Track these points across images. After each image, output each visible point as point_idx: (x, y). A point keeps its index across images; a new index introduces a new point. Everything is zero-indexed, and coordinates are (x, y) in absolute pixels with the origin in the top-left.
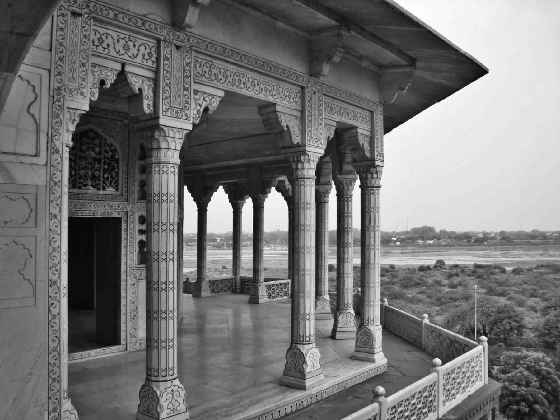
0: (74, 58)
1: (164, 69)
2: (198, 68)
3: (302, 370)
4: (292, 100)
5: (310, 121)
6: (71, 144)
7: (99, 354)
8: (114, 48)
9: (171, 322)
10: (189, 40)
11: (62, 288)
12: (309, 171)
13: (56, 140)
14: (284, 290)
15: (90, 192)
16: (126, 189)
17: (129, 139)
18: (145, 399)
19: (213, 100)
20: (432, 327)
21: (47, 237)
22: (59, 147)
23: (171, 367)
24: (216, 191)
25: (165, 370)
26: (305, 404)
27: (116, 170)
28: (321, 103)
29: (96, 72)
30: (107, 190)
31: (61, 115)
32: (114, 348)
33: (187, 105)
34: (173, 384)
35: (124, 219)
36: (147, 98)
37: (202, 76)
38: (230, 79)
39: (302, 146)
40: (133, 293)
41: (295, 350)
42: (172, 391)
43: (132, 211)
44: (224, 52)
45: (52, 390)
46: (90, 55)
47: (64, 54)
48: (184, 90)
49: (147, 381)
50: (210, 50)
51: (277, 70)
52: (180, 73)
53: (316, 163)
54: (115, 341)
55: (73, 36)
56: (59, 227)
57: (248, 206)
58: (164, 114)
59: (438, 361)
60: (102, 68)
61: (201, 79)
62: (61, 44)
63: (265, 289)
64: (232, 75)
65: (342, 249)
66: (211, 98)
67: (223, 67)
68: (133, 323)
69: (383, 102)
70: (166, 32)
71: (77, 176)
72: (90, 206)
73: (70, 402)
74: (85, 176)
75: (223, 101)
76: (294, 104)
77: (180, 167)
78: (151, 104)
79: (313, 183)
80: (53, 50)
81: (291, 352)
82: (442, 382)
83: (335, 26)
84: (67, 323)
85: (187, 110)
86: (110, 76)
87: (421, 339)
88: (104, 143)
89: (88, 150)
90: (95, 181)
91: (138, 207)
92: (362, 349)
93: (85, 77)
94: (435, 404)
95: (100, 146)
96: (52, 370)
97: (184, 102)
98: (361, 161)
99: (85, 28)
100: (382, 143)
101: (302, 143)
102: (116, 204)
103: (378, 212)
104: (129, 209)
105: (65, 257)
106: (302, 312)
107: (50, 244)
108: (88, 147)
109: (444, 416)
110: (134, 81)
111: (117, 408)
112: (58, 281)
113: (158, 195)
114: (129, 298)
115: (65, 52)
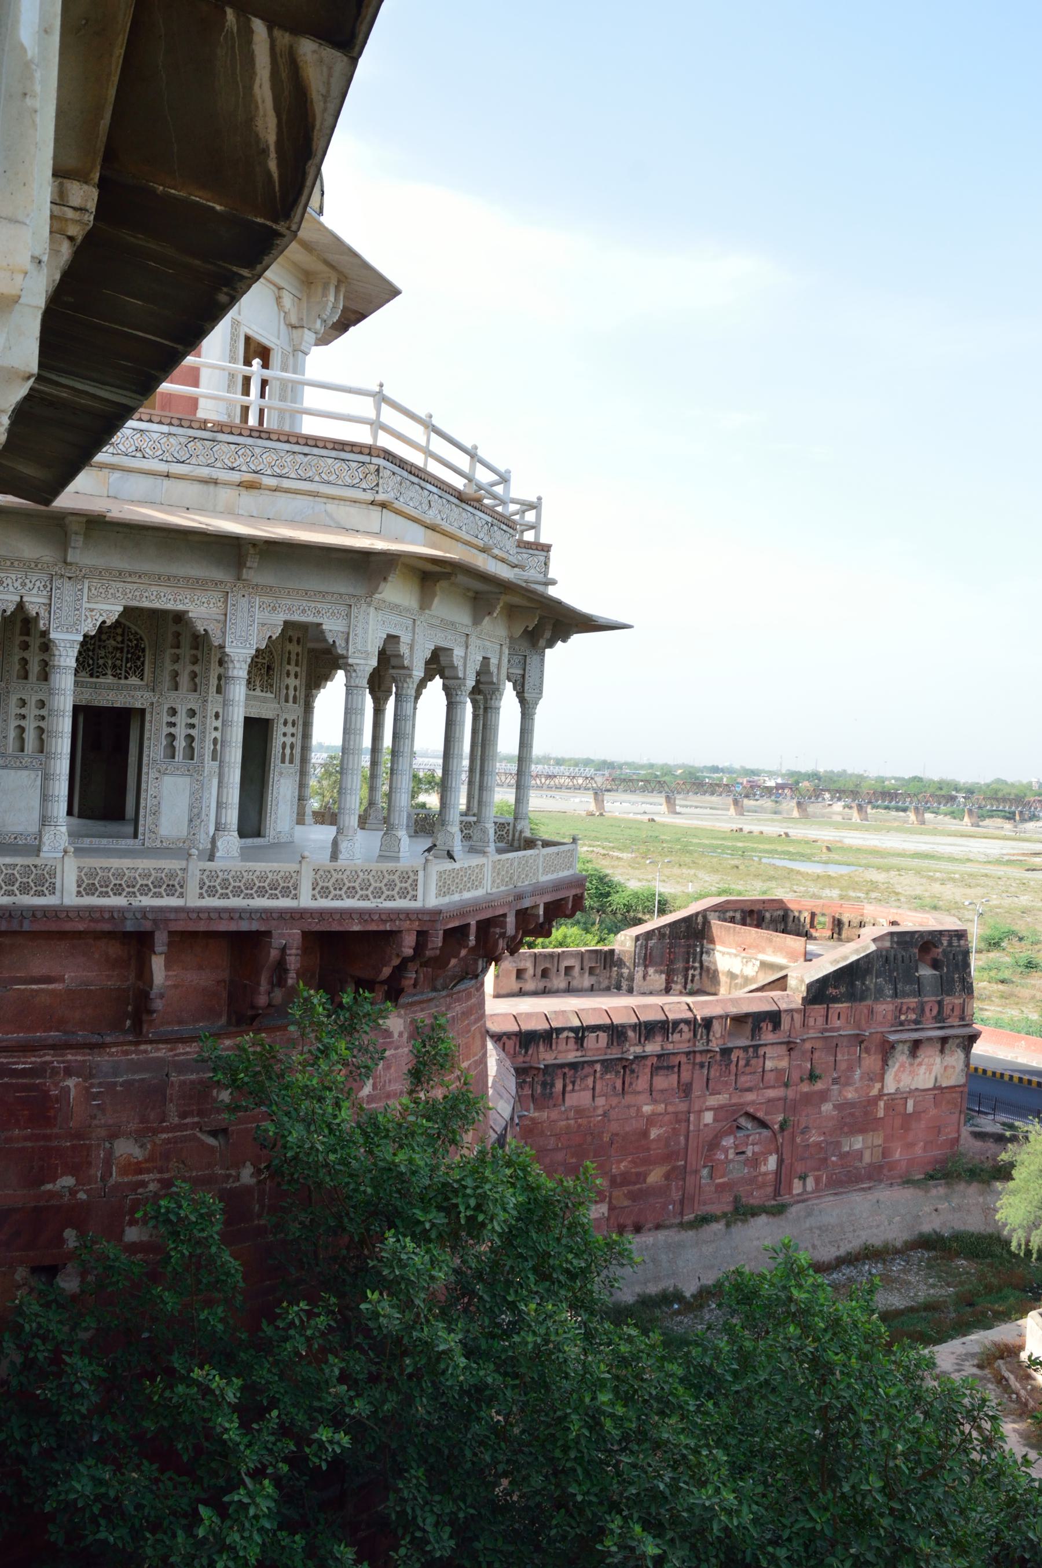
95: (122, 635)
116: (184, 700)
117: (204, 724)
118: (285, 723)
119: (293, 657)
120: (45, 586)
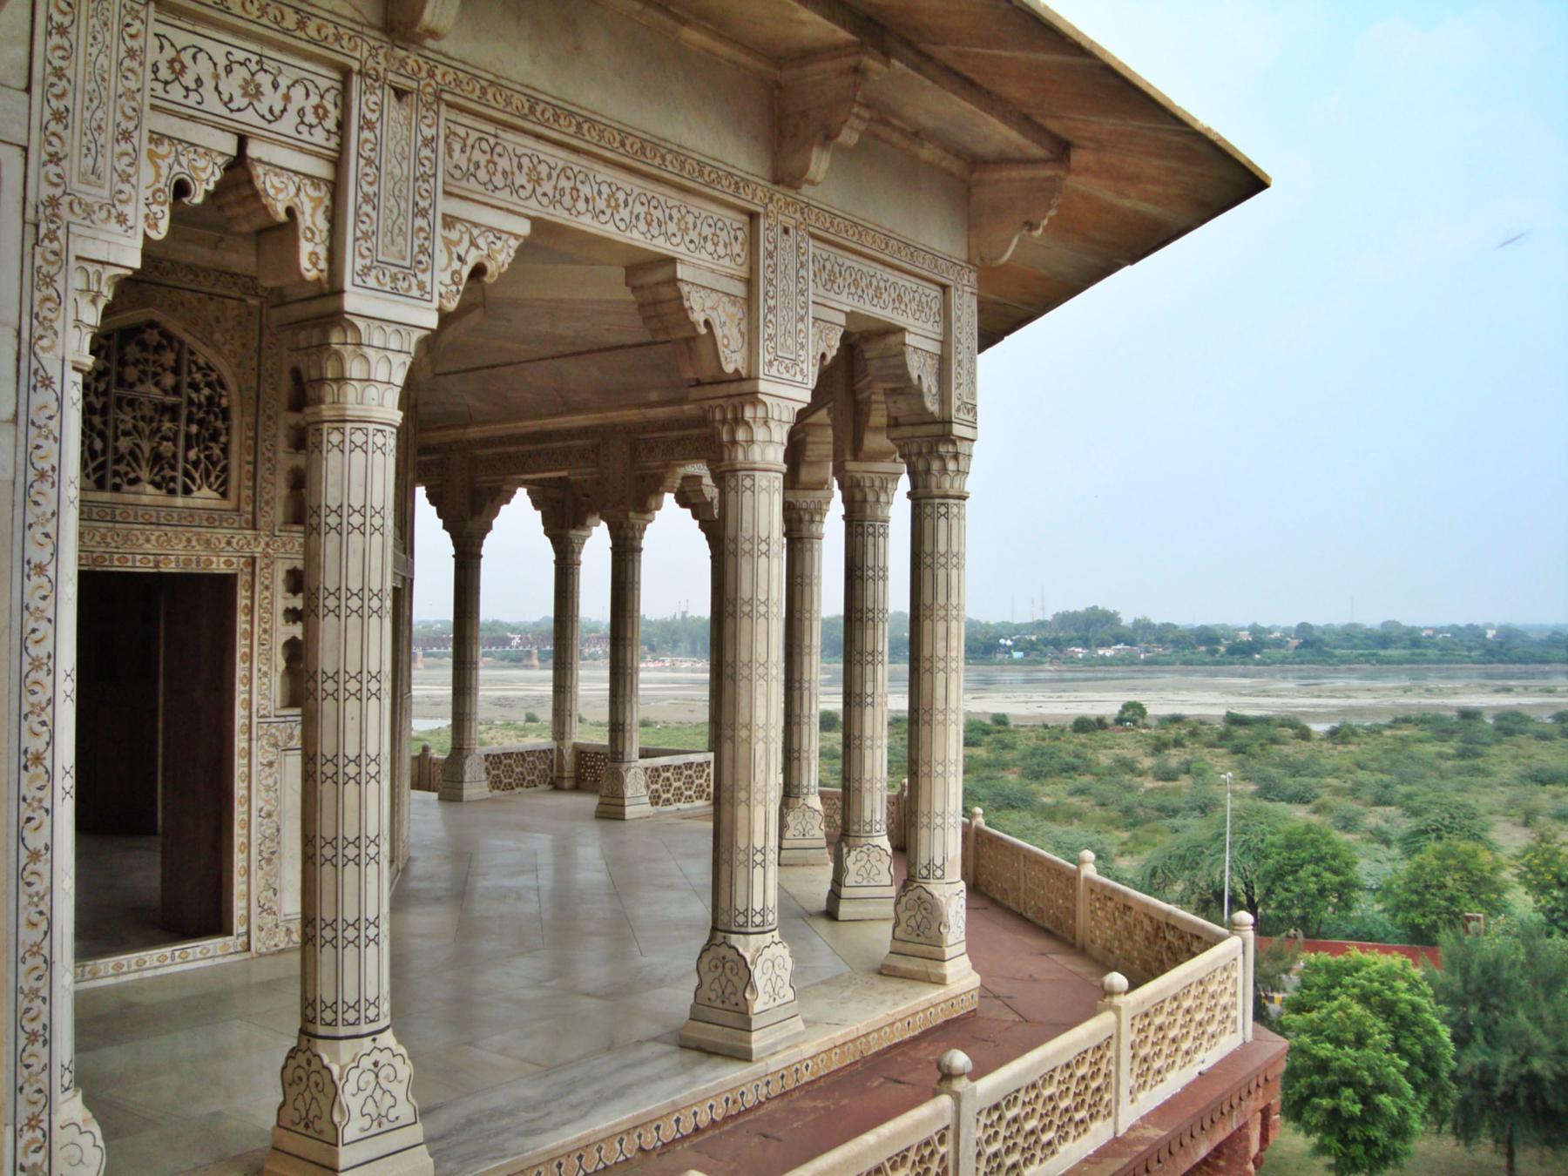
0: (99, 114)
1: (359, 154)
2: (457, 154)
3: (742, 1004)
4: (721, 250)
5: (770, 310)
6: (89, 361)
7: (169, 961)
8: (216, 88)
9: (372, 869)
10: (431, 75)
11: (59, 773)
12: (767, 448)
13: (43, 349)
14: (698, 782)
15: (145, 499)
16: (250, 493)
17: (259, 351)
18: (295, 1090)
19: (499, 244)
20: (1104, 887)
21: (16, 625)
22: (54, 370)
23: (371, 996)
24: (508, 502)
25: (356, 1006)
26: (750, 1100)
27: (223, 439)
28: (803, 259)
29: (163, 157)
30: (196, 494)
31: (60, 278)
32: (213, 944)
33: (424, 258)
34: (378, 1044)
35: (243, 580)
36: (309, 235)
38: (548, 187)
39: (749, 378)
40: (268, 788)
41: (723, 950)
42: (376, 1064)
43: (266, 556)
44: (532, 110)
45: (28, 1066)
46: (147, 108)
47: (68, 101)
48: (415, 215)
49: (305, 1038)
50: (493, 103)
51: (682, 164)
52: (405, 166)
53: (787, 427)
54: (215, 922)
55: (94, 51)
56: (51, 600)
57: (597, 545)
58: (358, 281)
59: (1117, 979)
60: (180, 148)
61: (464, 183)
62: (59, 73)
63: (643, 779)
64: (554, 175)
65: (857, 670)
67: (529, 152)
68: (267, 874)
69: (977, 261)
70: (366, 47)
71: (110, 457)
72: (148, 540)
73: (80, 1095)
75: (527, 249)
76: (726, 262)
77: (402, 433)
78: (322, 252)
79: (778, 482)
80: (37, 90)
81: (710, 954)
82: (1129, 1036)
83: (848, 44)
84: (72, 872)
85: (424, 271)
86: (204, 170)
87: (1074, 919)
88: (190, 361)
89: (141, 381)
90: (161, 469)
91: (284, 545)
92: (910, 948)
93: (131, 170)
94: (1107, 1097)
95: (176, 371)
96: (28, 1010)
97: (416, 249)
98: (913, 424)
99: (132, 30)
100: (972, 373)
101: (749, 371)
102: (221, 534)
103: (959, 567)
105: (67, 686)
106: (742, 843)
107: (24, 647)
108: (144, 372)
109: (1132, 1128)
110: (273, 186)
111: (219, 1114)
112: (48, 754)
113: (338, 511)
115: (70, 95)
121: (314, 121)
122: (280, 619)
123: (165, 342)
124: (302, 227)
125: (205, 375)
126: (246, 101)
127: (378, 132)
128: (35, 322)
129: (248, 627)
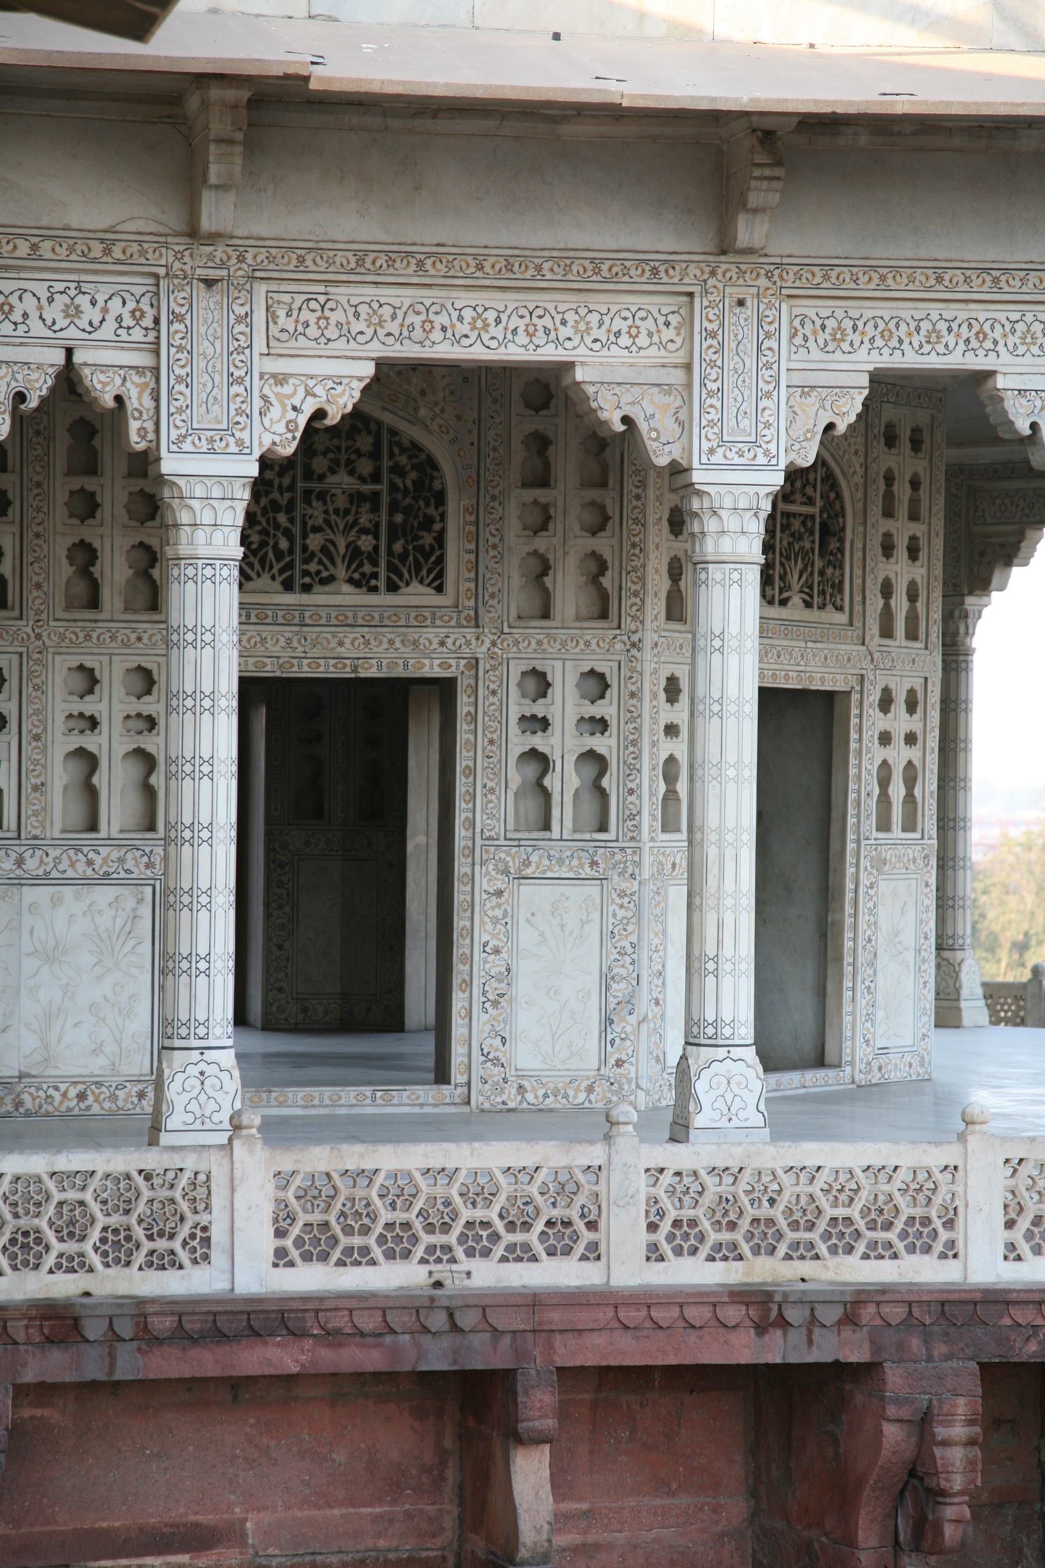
8: (41, 317)
10: (241, 259)
16: (472, 585)
17: (478, 422)
19: (340, 389)
27: (437, 526)
33: (242, 419)
36: (136, 414)
37: (295, 335)
40: (495, 921)
52: (218, 345)
58: (173, 448)
60: (15, 368)
61: (293, 343)
66: (330, 384)
67: (368, 299)
70: (171, 253)
74: (324, 550)
76: (653, 351)
78: (150, 426)
85: (242, 430)
89: (333, 472)
91: (517, 643)
95: (375, 455)
97: (232, 413)
102: (431, 635)
104: (484, 649)
110: (100, 382)
114: (481, 936)
116: (569, 652)
117: (634, 717)
118: (886, 703)
119: (903, 491)
120: (137, 315)
121: (132, 323)
122: (514, 728)
123: (360, 425)
124: (129, 408)
125: (410, 457)
126: (68, 321)
127: (188, 322)
128: (248, 412)
129: (472, 737)
